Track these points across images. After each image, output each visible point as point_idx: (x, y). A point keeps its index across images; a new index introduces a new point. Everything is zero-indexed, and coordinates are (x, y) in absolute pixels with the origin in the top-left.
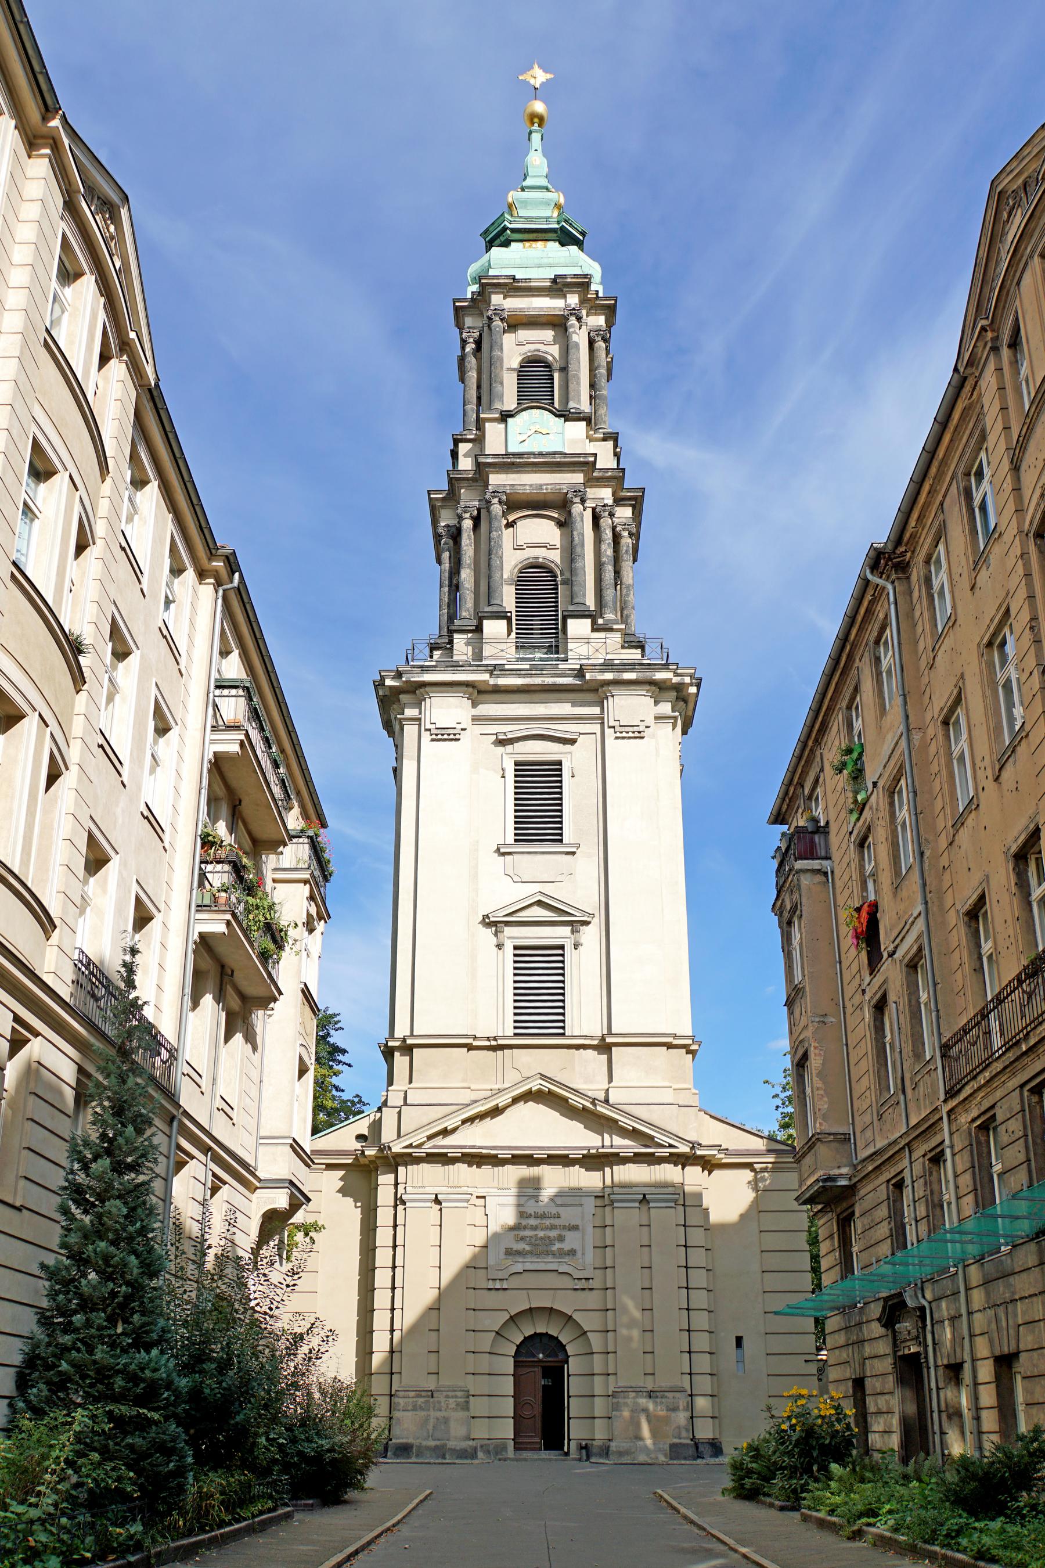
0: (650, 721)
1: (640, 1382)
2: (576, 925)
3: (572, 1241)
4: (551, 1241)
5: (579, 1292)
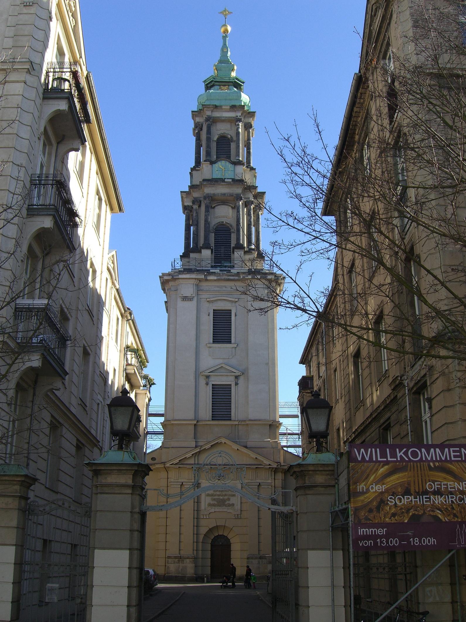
3: (233, 500)
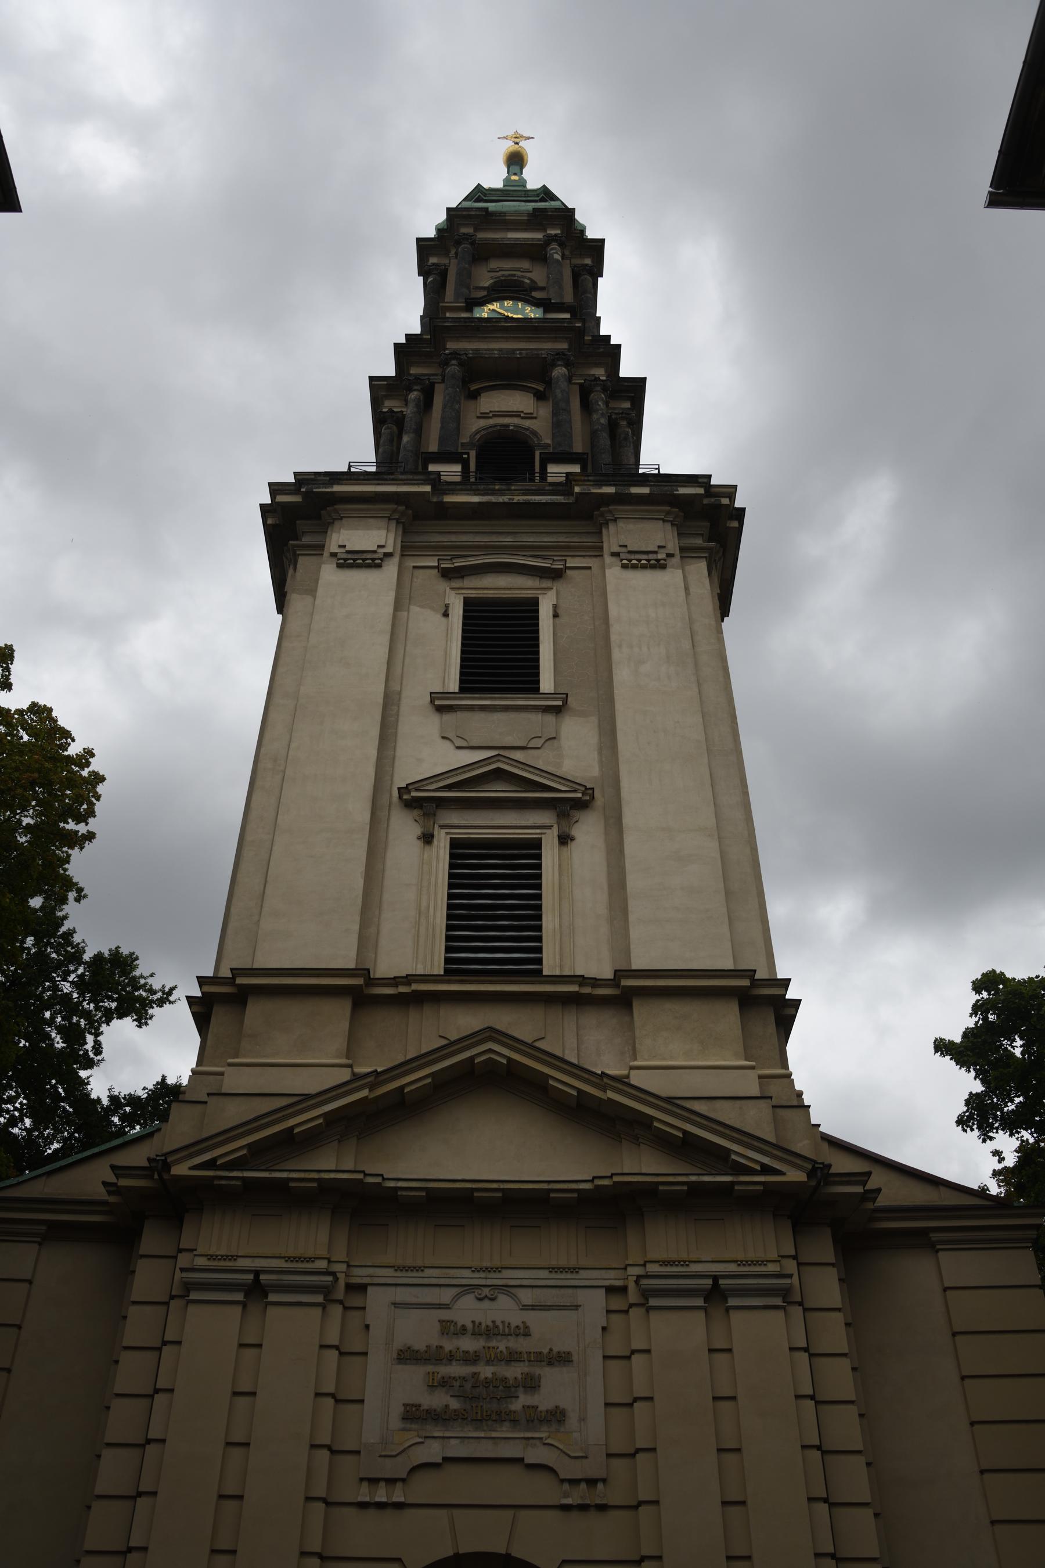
3: (555, 1389)
4: (508, 1389)
5: (575, 1514)
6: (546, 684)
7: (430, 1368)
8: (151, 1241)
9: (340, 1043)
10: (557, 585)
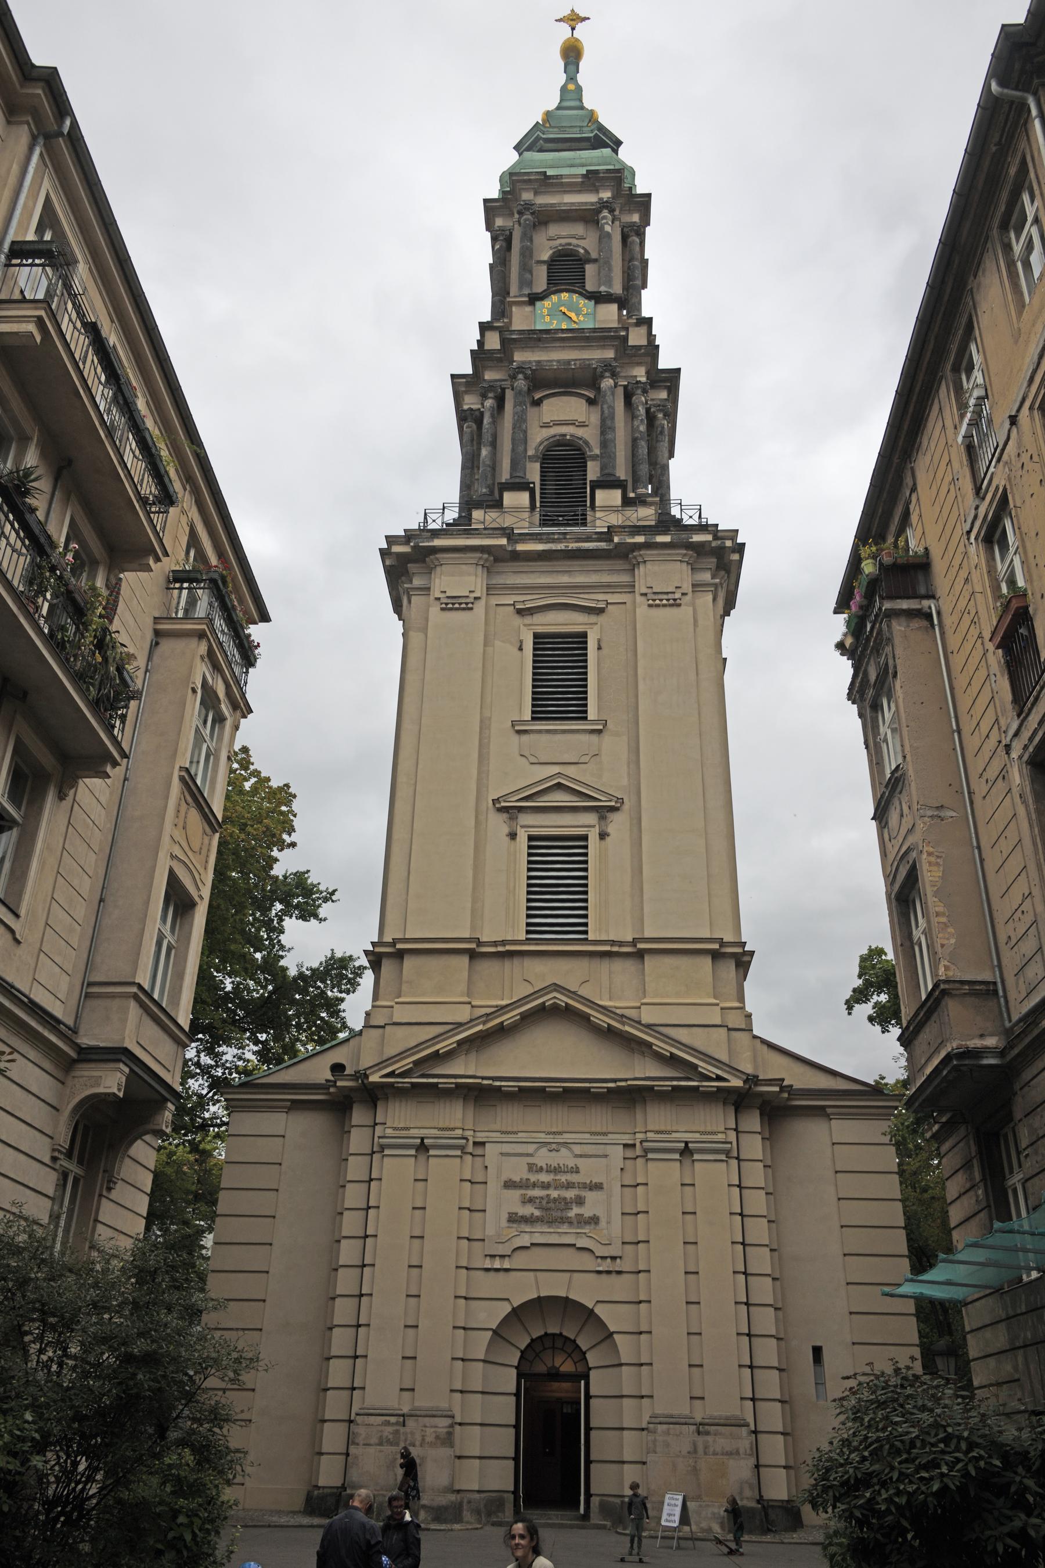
0: (687, 587)
1: (683, 1408)
2: (604, 812)
4: (567, 1204)
6: (592, 714)
7: (523, 1192)
8: (359, 1116)
9: (463, 987)
10: (601, 619)
